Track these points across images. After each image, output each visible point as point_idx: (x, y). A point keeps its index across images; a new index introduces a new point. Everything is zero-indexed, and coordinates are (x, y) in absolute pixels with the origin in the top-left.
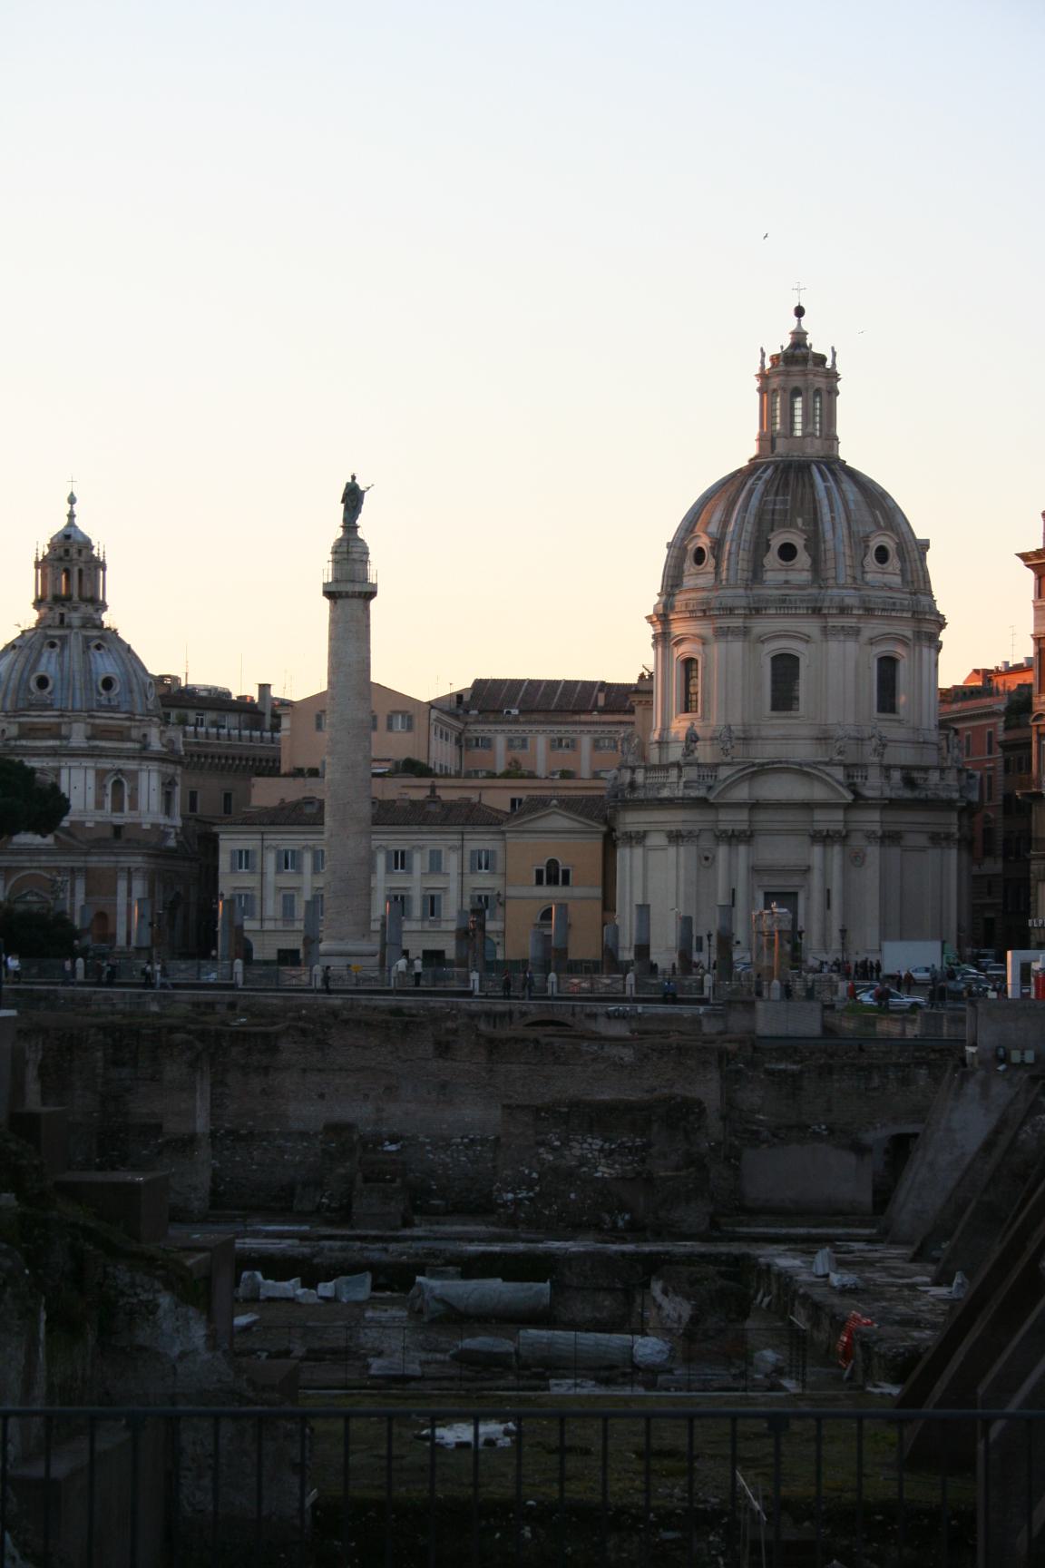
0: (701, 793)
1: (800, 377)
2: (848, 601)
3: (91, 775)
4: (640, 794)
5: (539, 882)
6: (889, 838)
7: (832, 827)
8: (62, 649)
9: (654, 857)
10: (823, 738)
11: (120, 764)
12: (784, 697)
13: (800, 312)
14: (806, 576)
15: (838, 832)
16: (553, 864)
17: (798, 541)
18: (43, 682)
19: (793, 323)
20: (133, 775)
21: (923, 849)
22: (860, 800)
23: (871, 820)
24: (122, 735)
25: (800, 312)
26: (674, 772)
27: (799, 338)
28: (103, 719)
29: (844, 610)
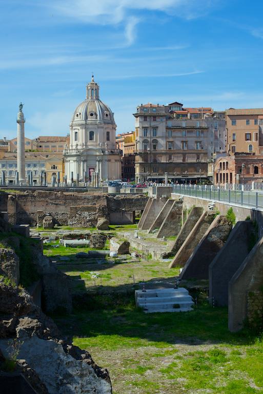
0: (79, 154)
6: (109, 161)
12: (91, 139)
13: (93, 76)
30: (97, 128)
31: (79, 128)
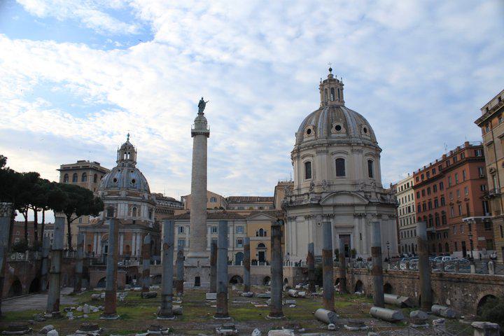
0: (316, 202)
1: (332, 88)
2: (359, 142)
3: (127, 207)
5: (257, 235)
6: (379, 216)
7: (362, 212)
10: (355, 184)
11: (135, 203)
13: (331, 70)
14: (345, 135)
16: (261, 230)
17: (342, 125)
18: (115, 180)
19: (329, 73)
20: (140, 206)
21: (387, 220)
22: (370, 204)
23: (374, 210)
25: (331, 70)
26: (306, 197)
27: (331, 76)
28: (132, 190)
30: (349, 152)
31: (313, 152)
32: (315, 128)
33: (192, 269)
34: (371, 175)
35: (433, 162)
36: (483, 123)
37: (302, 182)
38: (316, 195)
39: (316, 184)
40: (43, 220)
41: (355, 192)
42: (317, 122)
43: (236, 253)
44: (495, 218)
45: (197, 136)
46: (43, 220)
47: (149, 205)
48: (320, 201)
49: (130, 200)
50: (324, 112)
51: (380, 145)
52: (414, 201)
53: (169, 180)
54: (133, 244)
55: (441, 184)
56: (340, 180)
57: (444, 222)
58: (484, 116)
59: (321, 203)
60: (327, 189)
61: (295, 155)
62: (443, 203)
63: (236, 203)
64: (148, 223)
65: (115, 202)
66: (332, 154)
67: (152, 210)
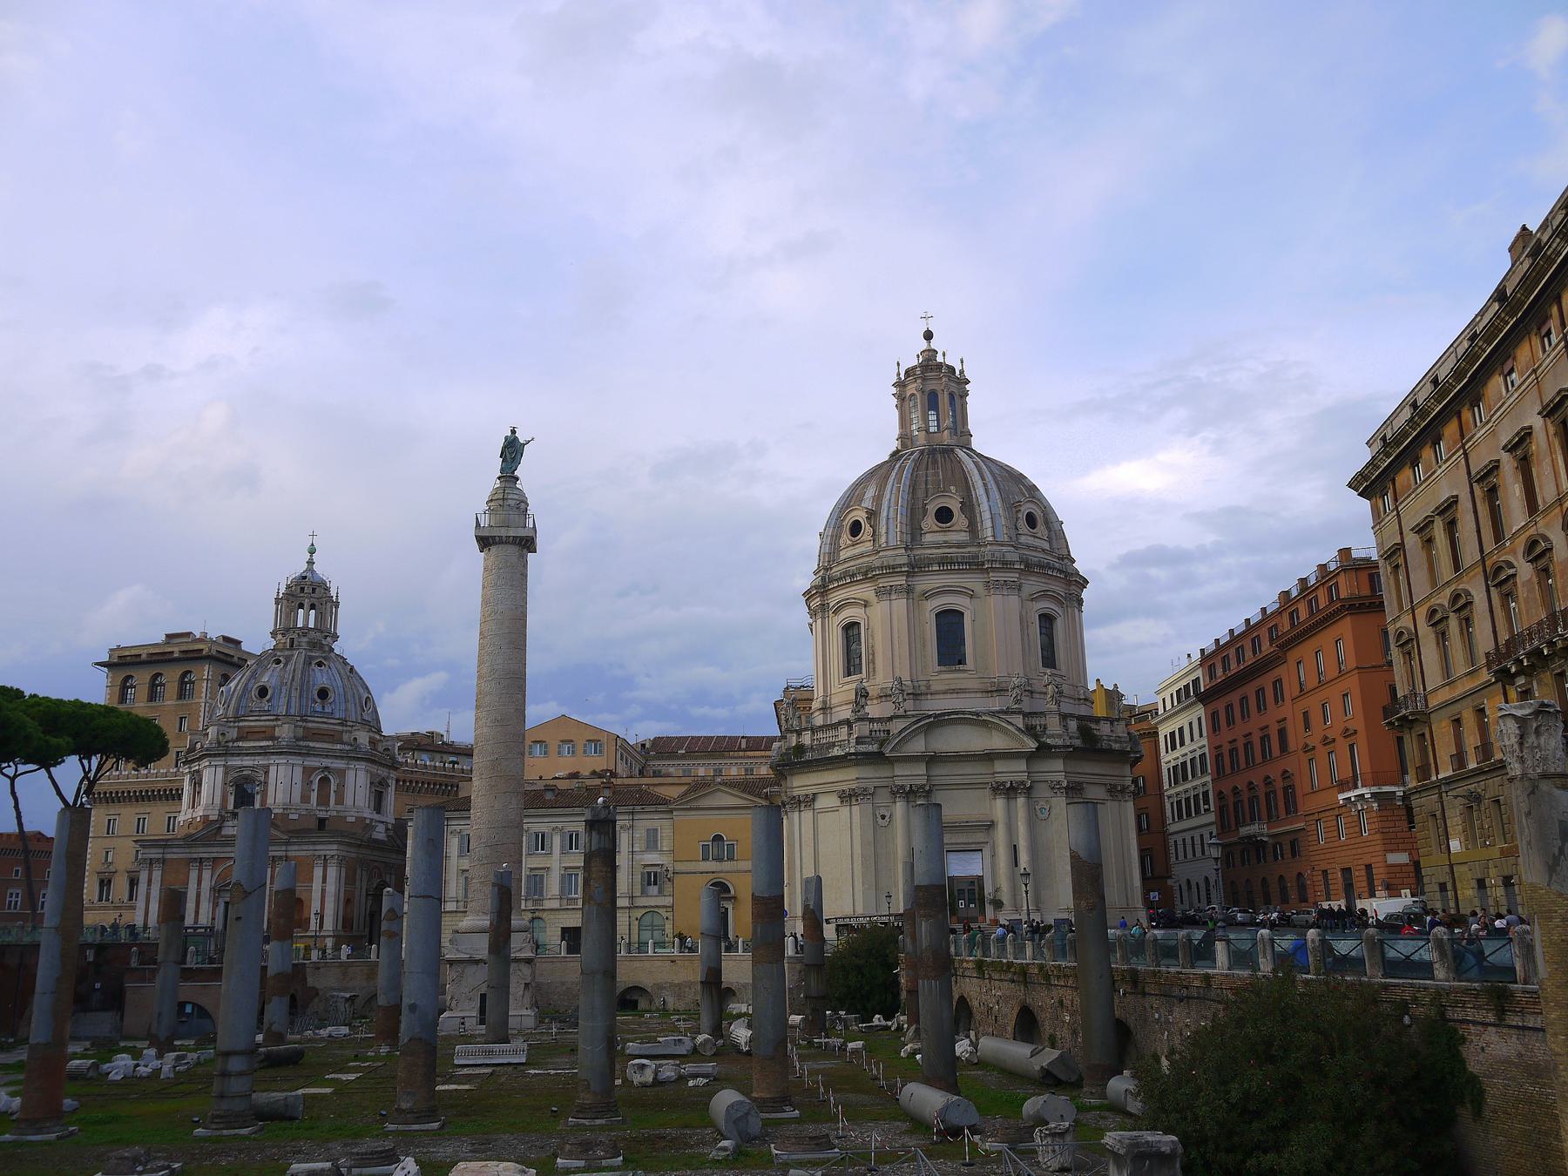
0: (874, 748)
1: (934, 388)
2: (1009, 557)
3: (298, 771)
4: (809, 756)
8: (286, 665)
9: (824, 820)
11: (327, 762)
13: (928, 336)
14: (963, 537)
15: (1023, 783)
17: (955, 506)
18: (263, 692)
19: (924, 345)
20: (341, 773)
22: (1044, 751)
23: (1055, 769)
24: (333, 737)
25: (928, 336)
26: (844, 730)
29: (1006, 565)
31: (865, 591)
32: (872, 515)
33: (471, 969)
34: (1049, 660)
35: (1254, 614)
36: (1371, 484)
37: (835, 688)
38: (876, 726)
39: (873, 692)
40: (20, 824)
41: (993, 714)
42: (878, 499)
43: (639, 914)
44: (1417, 791)
45: (493, 549)
46: (20, 824)
47: (374, 768)
48: (882, 743)
49: (309, 753)
50: (902, 469)
51: (1081, 566)
52: (1205, 742)
53: (421, 687)
54: (316, 895)
55: (1278, 683)
56: (949, 678)
57: (1291, 805)
58: (1372, 464)
59: (887, 751)
60: (909, 705)
61: (816, 602)
62: (1284, 747)
63: (672, 755)
64: (369, 827)
65: (261, 761)
66: (926, 596)
67: (383, 783)
